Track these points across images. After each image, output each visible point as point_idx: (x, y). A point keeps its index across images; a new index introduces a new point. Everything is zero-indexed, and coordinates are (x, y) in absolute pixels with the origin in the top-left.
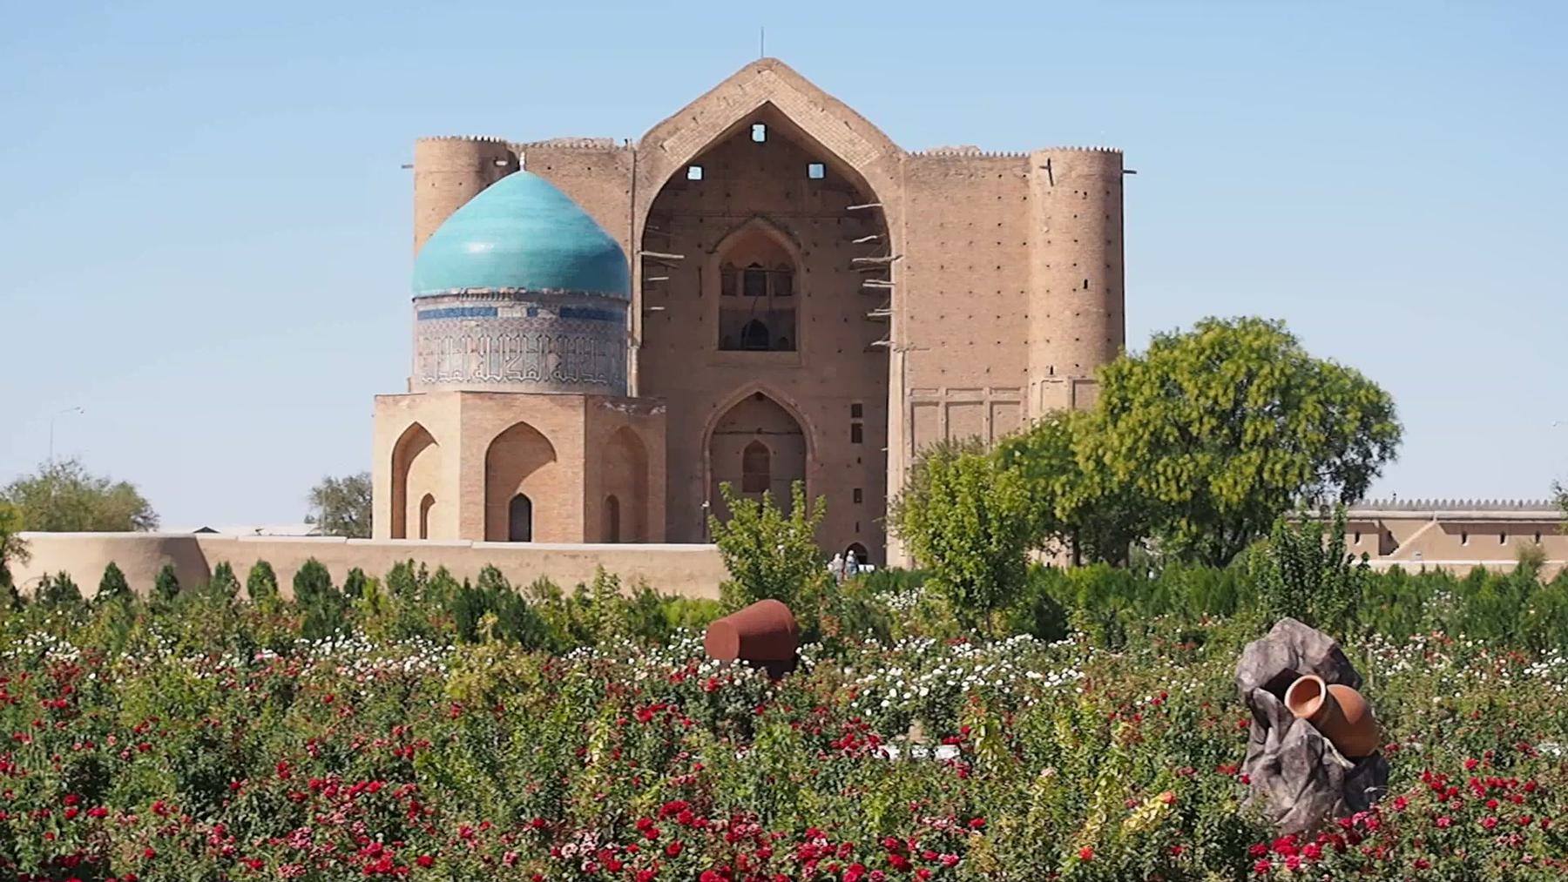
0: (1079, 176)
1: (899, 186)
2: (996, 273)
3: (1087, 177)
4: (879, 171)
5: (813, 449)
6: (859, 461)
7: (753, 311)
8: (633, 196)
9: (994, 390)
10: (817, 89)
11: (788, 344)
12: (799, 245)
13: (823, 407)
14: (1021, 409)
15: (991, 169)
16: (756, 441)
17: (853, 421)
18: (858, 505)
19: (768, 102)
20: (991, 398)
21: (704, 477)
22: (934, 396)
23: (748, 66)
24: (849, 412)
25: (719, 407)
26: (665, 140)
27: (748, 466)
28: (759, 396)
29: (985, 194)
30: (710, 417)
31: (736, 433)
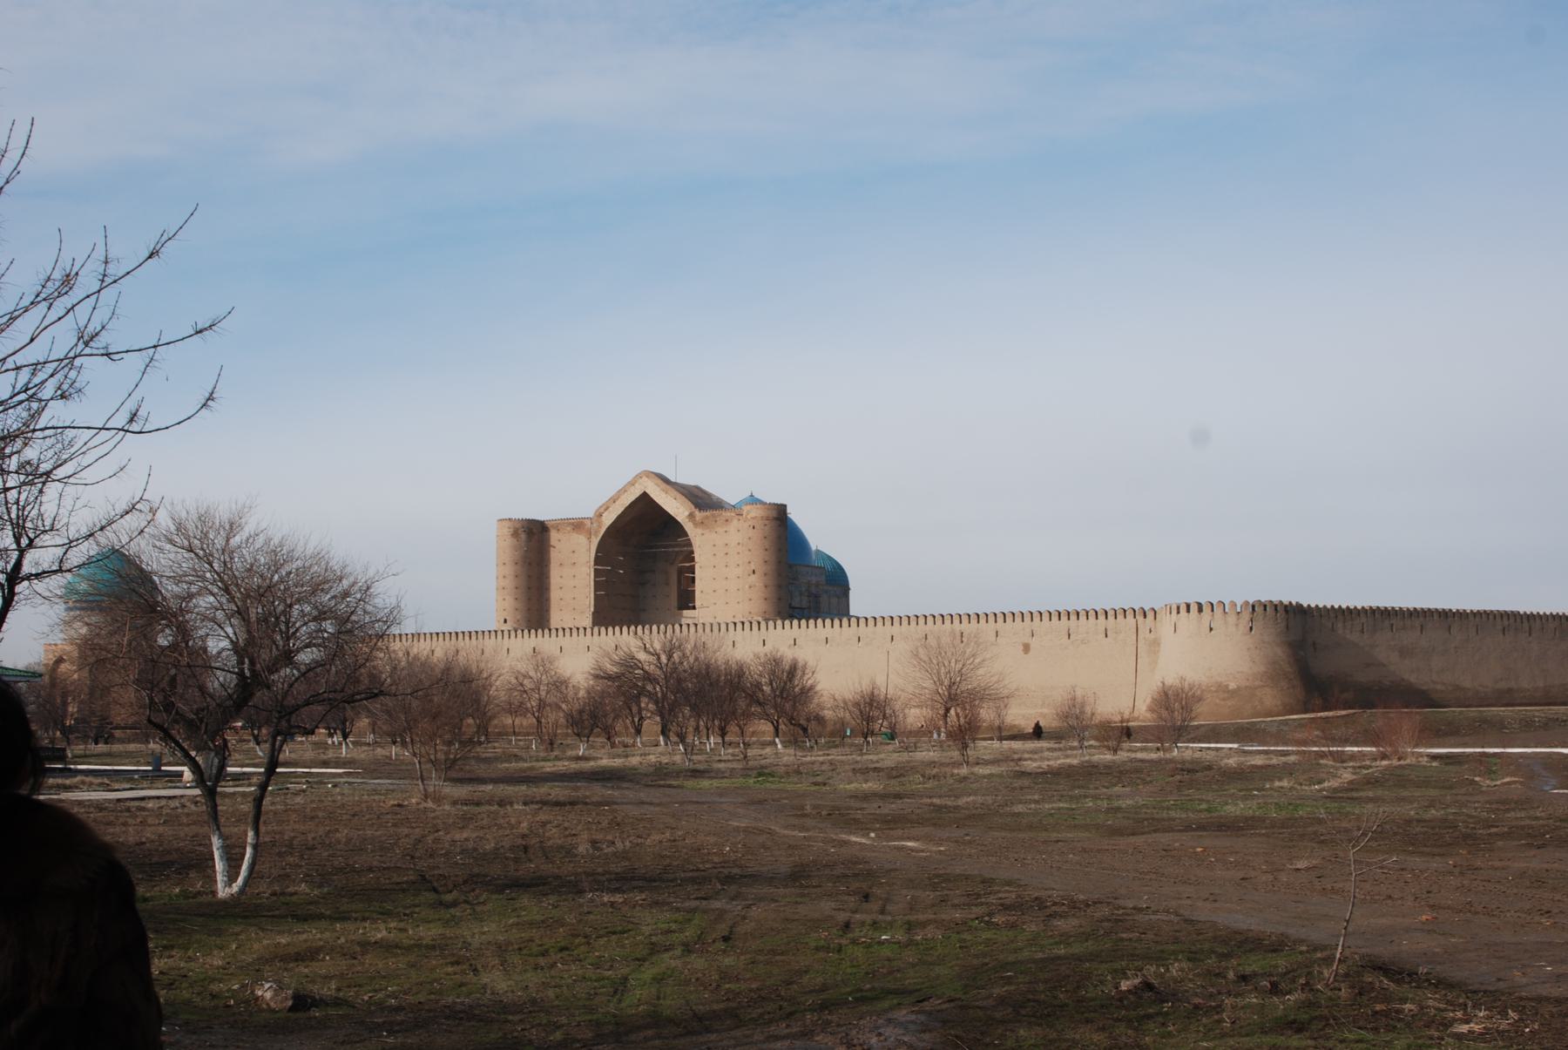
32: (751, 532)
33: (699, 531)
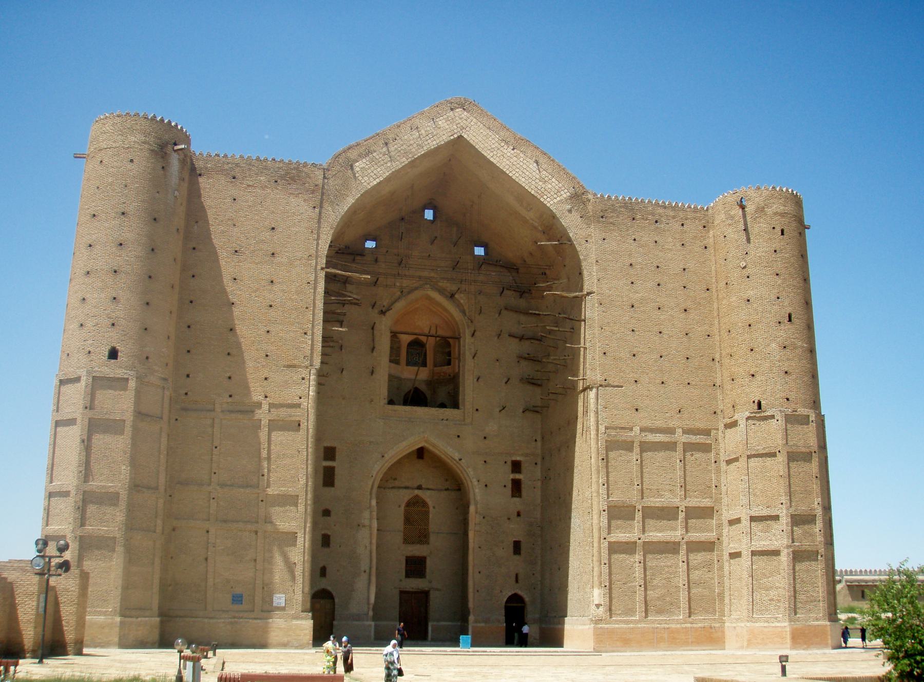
0: (776, 214)
1: (589, 225)
2: (683, 315)
3: (783, 215)
6: (519, 514)
7: (415, 379)
8: (320, 213)
9: (686, 432)
11: (454, 402)
14: (713, 454)
15: (674, 217)
16: (417, 496)
17: (512, 476)
18: (517, 557)
19: (460, 137)
20: (685, 439)
21: (370, 527)
24: (509, 467)
27: (408, 520)
29: (670, 239)
30: (377, 467)
32: (778, 242)
33: (595, 232)
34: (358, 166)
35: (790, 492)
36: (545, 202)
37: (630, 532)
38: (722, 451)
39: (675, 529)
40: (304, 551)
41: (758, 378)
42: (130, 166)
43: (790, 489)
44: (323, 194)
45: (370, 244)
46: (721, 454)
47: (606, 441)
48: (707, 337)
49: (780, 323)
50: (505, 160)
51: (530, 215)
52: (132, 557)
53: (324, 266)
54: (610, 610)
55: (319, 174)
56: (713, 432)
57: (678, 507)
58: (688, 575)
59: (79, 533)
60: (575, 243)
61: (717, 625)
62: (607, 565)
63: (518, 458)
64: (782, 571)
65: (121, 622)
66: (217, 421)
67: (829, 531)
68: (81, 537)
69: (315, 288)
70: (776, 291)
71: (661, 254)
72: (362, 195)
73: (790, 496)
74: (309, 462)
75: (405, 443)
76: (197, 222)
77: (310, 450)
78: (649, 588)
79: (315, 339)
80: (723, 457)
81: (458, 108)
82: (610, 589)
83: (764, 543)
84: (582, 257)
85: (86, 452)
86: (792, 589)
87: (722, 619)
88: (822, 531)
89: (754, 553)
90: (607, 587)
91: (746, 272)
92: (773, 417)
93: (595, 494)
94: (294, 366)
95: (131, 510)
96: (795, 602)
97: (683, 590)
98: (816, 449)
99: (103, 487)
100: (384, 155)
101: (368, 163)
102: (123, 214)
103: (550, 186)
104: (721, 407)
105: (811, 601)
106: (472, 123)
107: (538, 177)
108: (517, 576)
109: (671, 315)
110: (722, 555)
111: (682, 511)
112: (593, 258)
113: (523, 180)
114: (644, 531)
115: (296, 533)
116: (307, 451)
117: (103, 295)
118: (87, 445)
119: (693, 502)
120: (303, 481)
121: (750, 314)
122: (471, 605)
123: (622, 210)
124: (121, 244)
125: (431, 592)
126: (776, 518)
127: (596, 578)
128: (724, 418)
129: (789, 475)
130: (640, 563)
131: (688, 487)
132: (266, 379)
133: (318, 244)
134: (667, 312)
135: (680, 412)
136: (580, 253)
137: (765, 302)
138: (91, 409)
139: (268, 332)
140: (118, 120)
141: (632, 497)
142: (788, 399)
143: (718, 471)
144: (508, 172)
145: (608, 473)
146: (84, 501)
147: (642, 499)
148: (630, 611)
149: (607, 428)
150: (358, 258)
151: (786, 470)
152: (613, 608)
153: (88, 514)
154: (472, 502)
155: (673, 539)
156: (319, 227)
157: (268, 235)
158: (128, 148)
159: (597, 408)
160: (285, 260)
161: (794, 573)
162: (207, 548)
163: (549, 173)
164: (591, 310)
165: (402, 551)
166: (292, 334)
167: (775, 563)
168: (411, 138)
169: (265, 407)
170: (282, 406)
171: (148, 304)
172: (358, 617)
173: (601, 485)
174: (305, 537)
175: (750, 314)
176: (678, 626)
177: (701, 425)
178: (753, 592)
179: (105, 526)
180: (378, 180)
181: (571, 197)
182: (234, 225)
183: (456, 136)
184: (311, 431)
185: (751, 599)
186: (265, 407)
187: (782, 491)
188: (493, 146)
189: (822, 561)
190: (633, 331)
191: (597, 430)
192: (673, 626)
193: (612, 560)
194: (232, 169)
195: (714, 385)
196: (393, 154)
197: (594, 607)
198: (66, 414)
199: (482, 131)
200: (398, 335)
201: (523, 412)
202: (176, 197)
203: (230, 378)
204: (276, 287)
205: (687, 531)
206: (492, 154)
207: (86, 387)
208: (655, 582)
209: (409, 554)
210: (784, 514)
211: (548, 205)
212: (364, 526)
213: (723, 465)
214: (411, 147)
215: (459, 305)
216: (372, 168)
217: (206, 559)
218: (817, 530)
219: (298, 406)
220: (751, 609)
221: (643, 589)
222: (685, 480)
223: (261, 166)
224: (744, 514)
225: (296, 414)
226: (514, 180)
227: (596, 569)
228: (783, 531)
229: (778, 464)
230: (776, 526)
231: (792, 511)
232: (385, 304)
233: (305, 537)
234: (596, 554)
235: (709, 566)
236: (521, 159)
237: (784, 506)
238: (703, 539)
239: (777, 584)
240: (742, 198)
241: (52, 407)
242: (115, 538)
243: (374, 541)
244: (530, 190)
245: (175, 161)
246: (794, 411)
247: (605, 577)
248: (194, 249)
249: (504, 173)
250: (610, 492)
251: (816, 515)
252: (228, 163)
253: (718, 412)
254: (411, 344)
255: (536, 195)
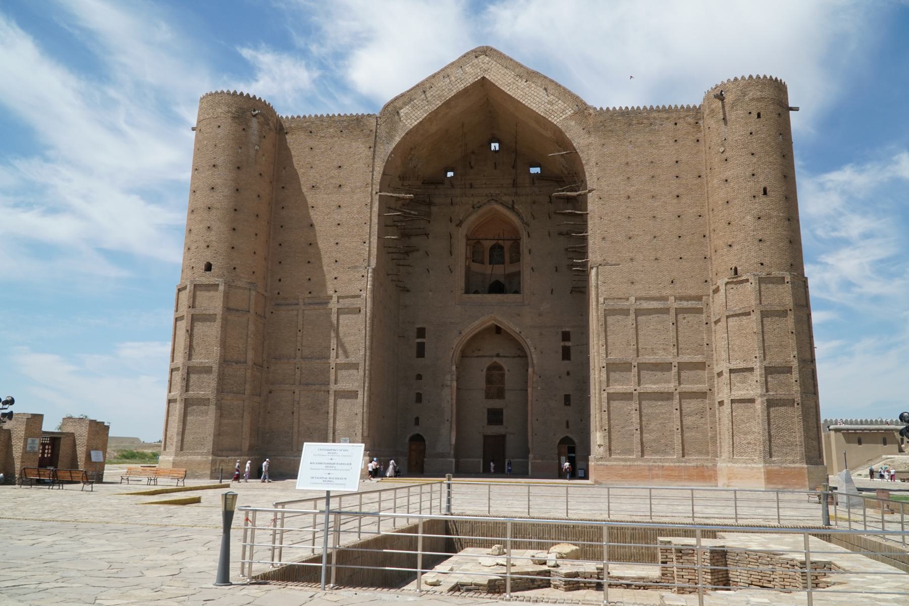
2: (675, 201)
3: (759, 100)
4: (573, 123)
5: (533, 366)
6: (568, 374)
8: (374, 151)
9: (681, 299)
10: (522, 66)
12: (522, 219)
13: (541, 334)
14: (704, 316)
15: (667, 119)
16: (495, 362)
17: (562, 344)
19: (484, 78)
20: (676, 305)
22: (624, 304)
23: (468, 53)
24: (560, 336)
25: (464, 334)
26: (402, 108)
27: (489, 381)
28: (498, 330)
29: (664, 138)
31: (482, 356)
34: (402, 112)
35: (764, 346)
36: (553, 121)
37: (627, 385)
38: (712, 313)
39: (669, 382)
40: (363, 405)
41: (735, 247)
42: (219, 130)
43: (764, 344)
44: (376, 136)
45: (450, 174)
46: (712, 317)
47: (605, 310)
48: (698, 217)
49: (754, 197)
50: (519, 91)
51: (548, 134)
52: (222, 412)
53: (378, 191)
54: (610, 449)
55: (373, 121)
56: (704, 298)
57: (671, 363)
58: (681, 421)
59: (184, 396)
60: (578, 151)
61: (710, 465)
62: (607, 412)
63: (567, 330)
64: (756, 418)
65: (212, 460)
66: (300, 311)
67: (812, 381)
68: (185, 399)
69: (371, 208)
70: (751, 169)
71: (655, 151)
72: (407, 134)
73: (764, 350)
74: (367, 338)
75: (477, 322)
76: (285, 168)
77: (368, 329)
78: (644, 431)
79: (372, 245)
80: (713, 319)
81: (481, 55)
82: (609, 432)
83: (742, 392)
84: (584, 162)
85: (190, 338)
86: (767, 434)
87: (714, 459)
88: (798, 381)
89: (733, 401)
90: (607, 431)
91: (724, 156)
92: (747, 280)
93: (596, 354)
94: (356, 267)
95: (221, 378)
96: (770, 446)
97: (677, 433)
98: (792, 308)
99: (201, 363)
100: (422, 101)
101: (410, 109)
102: (214, 166)
103: (556, 107)
104: (711, 276)
105: (788, 446)
106: (493, 66)
107: (546, 101)
108: (567, 422)
109: (664, 202)
110: (715, 404)
111: (675, 366)
112: (592, 163)
113: (534, 105)
114: (639, 384)
115: (358, 391)
116: (366, 329)
117: (201, 226)
118: (190, 333)
119: (685, 358)
120: (362, 352)
121: (728, 193)
122: (530, 446)
123: (620, 118)
124: (213, 188)
125: (507, 436)
126: (751, 370)
127: (598, 423)
128: (712, 285)
129: (763, 332)
130: (636, 410)
131: (680, 346)
132: (336, 278)
133: (373, 175)
134: (661, 199)
135: (672, 282)
136: (582, 159)
137: (741, 180)
138: (193, 308)
139: (337, 243)
140: (210, 98)
141: (630, 356)
142: (762, 264)
143: (709, 331)
144: (521, 101)
145: (606, 336)
146: (188, 373)
147: (638, 356)
148: (630, 451)
149: (605, 299)
150: (440, 186)
151: (760, 327)
152: (612, 448)
153: (191, 383)
154: (530, 365)
155: (666, 390)
156: (374, 161)
157: (336, 172)
158: (217, 117)
159: (597, 284)
160: (348, 189)
161: (769, 419)
162: (293, 405)
163: (556, 97)
164: (593, 205)
165: (480, 404)
166: (354, 244)
167: (751, 410)
168: (444, 84)
169: (335, 299)
170: (347, 297)
171: (234, 229)
172: (442, 455)
173: (601, 346)
174: (364, 394)
175: (728, 193)
176: (672, 464)
177: (692, 292)
178: (733, 436)
179: (203, 391)
180: (418, 121)
181: (576, 113)
182: (312, 167)
183: (479, 78)
184: (368, 314)
185: (731, 443)
186: (335, 299)
187: (756, 346)
188: (510, 82)
189: (798, 408)
190: (629, 217)
191: (597, 301)
192: (667, 464)
193: (611, 408)
194: (309, 126)
195: (705, 258)
196: (429, 99)
197: (597, 447)
198: (180, 314)
199: (500, 70)
200: (481, 241)
201: (571, 293)
202: (256, 150)
203: (310, 279)
204: (342, 210)
205: (680, 384)
206: (508, 88)
207: (190, 292)
208: (651, 427)
209: (490, 407)
210: (757, 365)
211: (555, 123)
212: (447, 386)
213: (713, 324)
214: (444, 92)
215: (518, 214)
216: (414, 112)
217: (293, 413)
218: (794, 380)
219: (359, 296)
220: (731, 451)
221: (639, 432)
222: (677, 339)
223: (332, 120)
224: (724, 367)
225: (358, 303)
226: (527, 107)
227: (597, 415)
228: (757, 381)
229: (752, 323)
230: (751, 377)
231: (766, 363)
232: (461, 218)
233: (364, 394)
234: (597, 403)
235: (701, 413)
236: (533, 89)
237: (758, 359)
238: (695, 390)
239: (754, 430)
240: (722, 91)
241: (174, 309)
242: (209, 399)
243: (454, 397)
244: (540, 113)
245: (254, 124)
246: (768, 274)
247: (605, 422)
248: (283, 188)
249: (519, 102)
250: (609, 352)
251: (792, 367)
252: (306, 122)
253: (709, 280)
254: (492, 248)
255: (544, 116)
